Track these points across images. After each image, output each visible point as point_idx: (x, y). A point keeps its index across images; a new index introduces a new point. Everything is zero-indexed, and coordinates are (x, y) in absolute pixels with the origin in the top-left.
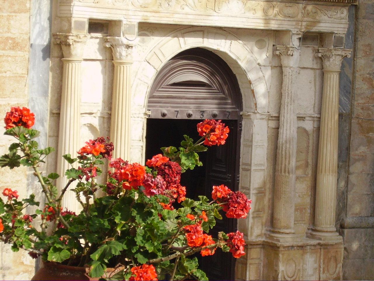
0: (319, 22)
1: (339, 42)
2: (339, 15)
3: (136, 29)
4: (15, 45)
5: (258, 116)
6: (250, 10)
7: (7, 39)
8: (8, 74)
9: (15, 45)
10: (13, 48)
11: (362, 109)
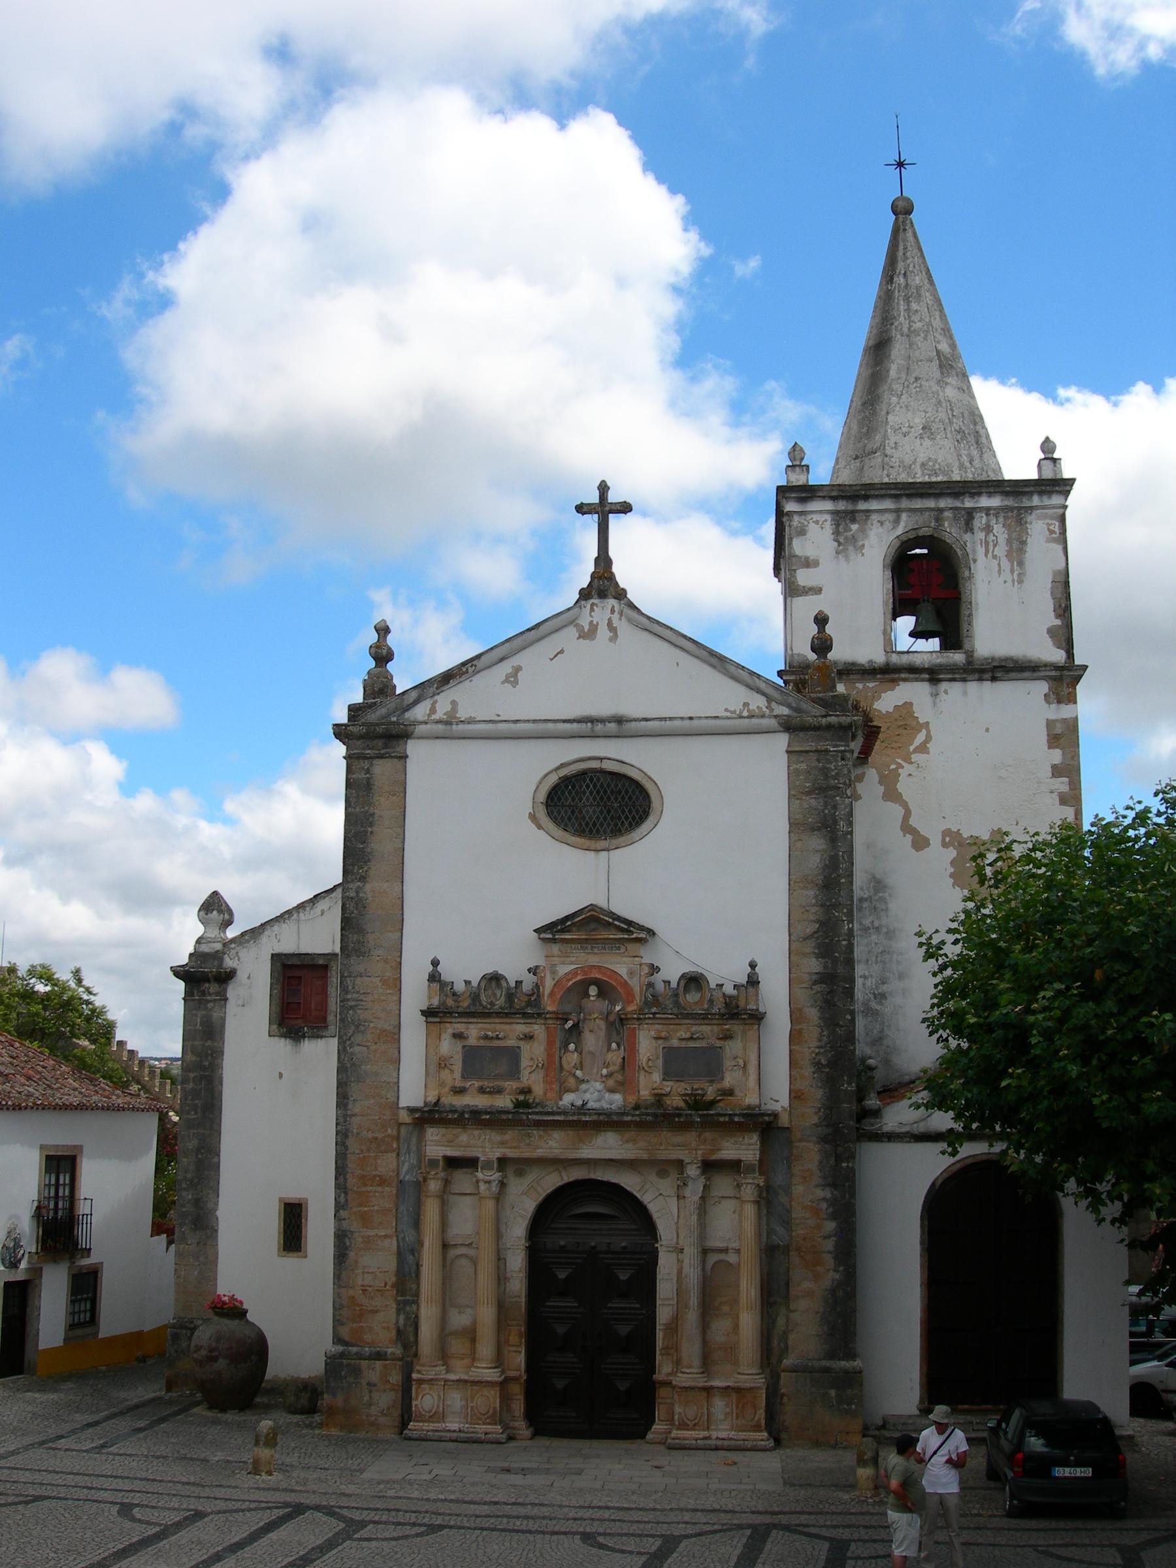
0: (719, 1150)
1: (750, 1169)
2: (746, 1141)
3: (495, 1165)
4: (382, 1181)
5: (664, 1249)
6: (627, 1142)
7: (375, 1176)
8: (376, 1208)
9: (382, 1181)
10: (380, 1185)
11: (804, 1239)
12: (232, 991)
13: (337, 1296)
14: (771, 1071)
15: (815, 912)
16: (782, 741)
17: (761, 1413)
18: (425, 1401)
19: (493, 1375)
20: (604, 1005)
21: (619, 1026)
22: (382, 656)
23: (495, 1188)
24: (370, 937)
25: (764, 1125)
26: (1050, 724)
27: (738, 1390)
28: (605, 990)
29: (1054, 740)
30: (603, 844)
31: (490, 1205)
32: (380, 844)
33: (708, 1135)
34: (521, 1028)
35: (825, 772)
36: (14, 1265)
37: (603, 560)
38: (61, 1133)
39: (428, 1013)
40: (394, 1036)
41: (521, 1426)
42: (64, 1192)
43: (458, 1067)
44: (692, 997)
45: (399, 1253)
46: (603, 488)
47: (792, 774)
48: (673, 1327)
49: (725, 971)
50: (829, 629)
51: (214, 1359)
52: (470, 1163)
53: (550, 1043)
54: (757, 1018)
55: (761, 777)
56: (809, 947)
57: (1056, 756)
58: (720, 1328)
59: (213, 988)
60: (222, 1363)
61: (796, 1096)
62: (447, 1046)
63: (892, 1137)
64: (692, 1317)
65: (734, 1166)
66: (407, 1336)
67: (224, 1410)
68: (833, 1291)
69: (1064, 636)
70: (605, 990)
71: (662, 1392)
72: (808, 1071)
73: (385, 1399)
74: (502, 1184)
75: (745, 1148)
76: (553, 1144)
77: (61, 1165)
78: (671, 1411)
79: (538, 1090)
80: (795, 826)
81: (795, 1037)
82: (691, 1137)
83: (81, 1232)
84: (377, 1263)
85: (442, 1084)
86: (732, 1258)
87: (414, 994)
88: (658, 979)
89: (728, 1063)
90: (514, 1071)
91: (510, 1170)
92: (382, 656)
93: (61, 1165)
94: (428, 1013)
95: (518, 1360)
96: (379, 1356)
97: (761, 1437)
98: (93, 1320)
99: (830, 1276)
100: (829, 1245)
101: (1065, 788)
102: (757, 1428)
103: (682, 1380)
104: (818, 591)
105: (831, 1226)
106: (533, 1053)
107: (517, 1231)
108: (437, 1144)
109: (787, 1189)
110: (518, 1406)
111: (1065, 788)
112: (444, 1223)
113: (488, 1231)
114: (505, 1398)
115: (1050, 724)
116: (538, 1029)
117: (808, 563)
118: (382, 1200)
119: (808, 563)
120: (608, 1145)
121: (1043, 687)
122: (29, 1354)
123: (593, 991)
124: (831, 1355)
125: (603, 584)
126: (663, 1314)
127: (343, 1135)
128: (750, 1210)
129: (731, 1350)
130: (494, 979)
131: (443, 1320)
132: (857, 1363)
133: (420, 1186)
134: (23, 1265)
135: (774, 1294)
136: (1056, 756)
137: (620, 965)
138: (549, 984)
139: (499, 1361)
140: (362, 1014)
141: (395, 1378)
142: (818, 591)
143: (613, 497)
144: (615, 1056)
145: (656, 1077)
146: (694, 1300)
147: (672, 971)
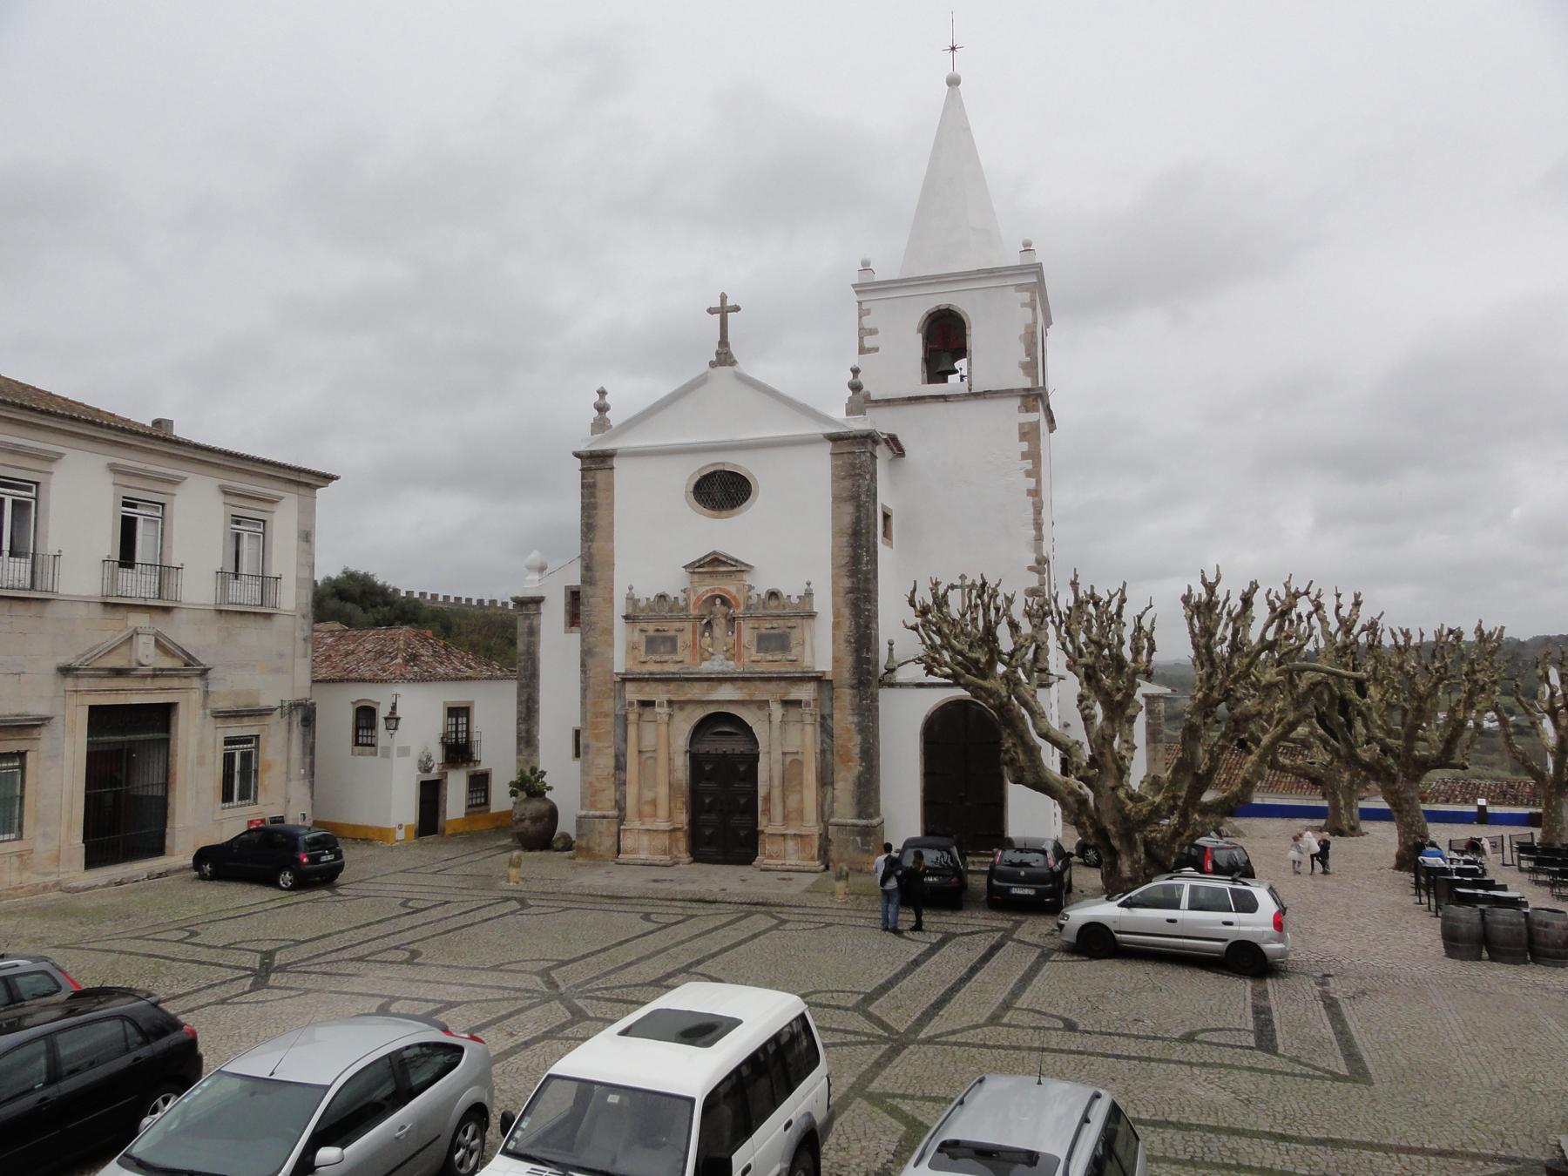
4: (606, 715)
9: (606, 715)
12: (543, 607)
13: (583, 781)
14: (821, 648)
15: (847, 551)
16: (828, 447)
17: (815, 851)
18: (628, 842)
19: (664, 826)
20: (723, 609)
21: (731, 621)
22: (602, 409)
23: (666, 718)
24: (597, 575)
25: (819, 679)
26: (1021, 426)
27: (801, 836)
28: (725, 601)
29: (1023, 436)
30: (725, 513)
31: (663, 728)
32: (601, 519)
33: (783, 684)
34: (678, 625)
35: (853, 466)
36: (428, 770)
37: (724, 342)
38: (457, 694)
39: (626, 617)
40: (609, 631)
41: (685, 857)
42: (462, 728)
43: (643, 649)
44: (773, 603)
45: (617, 757)
46: (723, 298)
47: (834, 467)
48: (768, 798)
49: (791, 589)
50: (861, 377)
51: (522, 820)
52: (650, 704)
53: (694, 632)
54: (811, 616)
55: (819, 469)
56: (844, 571)
57: (1025, 446)
58: (793, 801)
59: (532, 607)
60: (527, 823)
61: (836, 660)
62: (637, 636)
63: (901, 685)
64: (776, 793)
65: (798, 703)
66: (620, 805)
67: (530, 850)
68: (859, 778)
69: (1033, 365)
70: (725, 601)
71: (761, 837)
72: (843, 646)
73: (608, 842)
74: (670, 716)
75: (805, 693)
76: (696, 692)
77: (458, 712)
78: (767, 847)
79: (688, 660)
80: (837, 499)
81: (836, 626)
82: (772, 686)
83: (475, 750)
84: (606, 762)
85: (635, 658)
86: (799, 757)
87: (620, 607)
88: (753, 593)
89: (793, 642)
90: (674, 650)
91: (676, 707)
92: (602, 409)
93: (458, 712)
94: (626, 617)
95: (682, 819)
96: (604, 817)
97: (817, 865)
98: (487, 803)
99: (856, 768)
100: (857, 750)
101: (1030, 467)
102: (812, 859)
103: (768, 830)
104: (876, 350)
105: (858, 739)
106: (685, 638)
107: (681, 741)
108: (633, 693)
109: (831, 716)
110: (683, 844)
111: (1030, 467)
112: (639, 738)
113: (667, 743)
114: (673, 842)
115: (1021, 426)
116: (688, 626)
117: (873, 332)
118: (607, 725)
119: (873, 332)
120: (726, 693)
121: (1017, 402)
122: (441, 823)
123: (718, 601)
124: (859, 816)
125: (724, 357)
126: (762, 791)
127: (584, 690)
128: (809, 729)
129: (801, 813)
130: (662, 597)
131: (640, 796)
132: (875, 822)
133: (625, 717)
134: (435, 770)
135: (825, 780)
136: (1025, 446)
137: (731, 588)
138: (693, 598)
139: (670, 818)
140: (593, 619)
141: (614, 829)
142: (876, 350)
143: (730, 303)
144: (730, 640)
145: (753, 651)
146: (777, 781)
147: (762, 588)
